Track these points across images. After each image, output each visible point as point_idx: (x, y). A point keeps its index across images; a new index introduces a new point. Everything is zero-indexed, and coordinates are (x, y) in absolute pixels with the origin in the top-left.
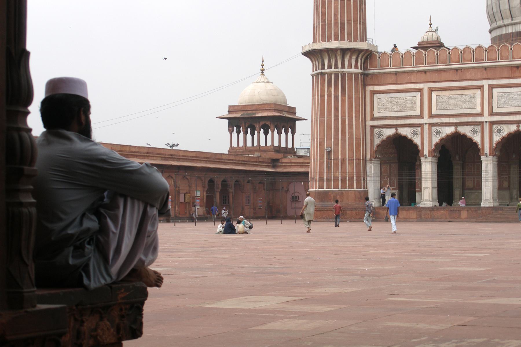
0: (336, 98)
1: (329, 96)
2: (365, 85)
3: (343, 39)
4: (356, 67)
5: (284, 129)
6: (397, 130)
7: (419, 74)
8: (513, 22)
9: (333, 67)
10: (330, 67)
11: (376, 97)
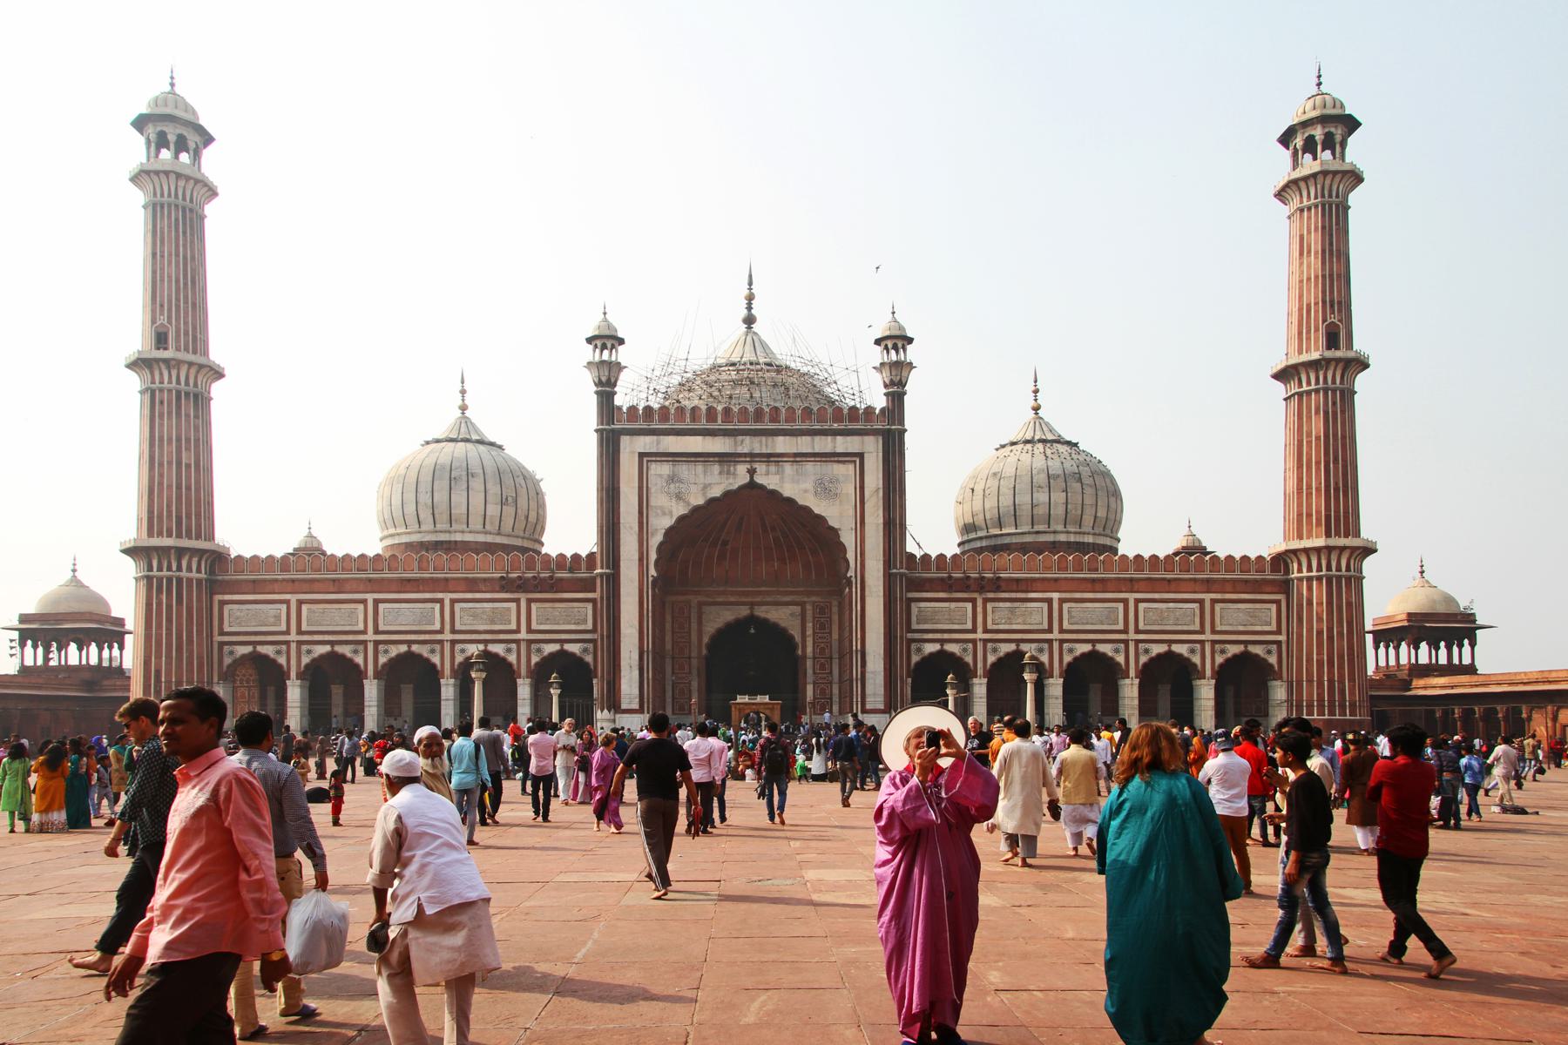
0: (169, 607)
2: (212, 594)
7: (284, 583)
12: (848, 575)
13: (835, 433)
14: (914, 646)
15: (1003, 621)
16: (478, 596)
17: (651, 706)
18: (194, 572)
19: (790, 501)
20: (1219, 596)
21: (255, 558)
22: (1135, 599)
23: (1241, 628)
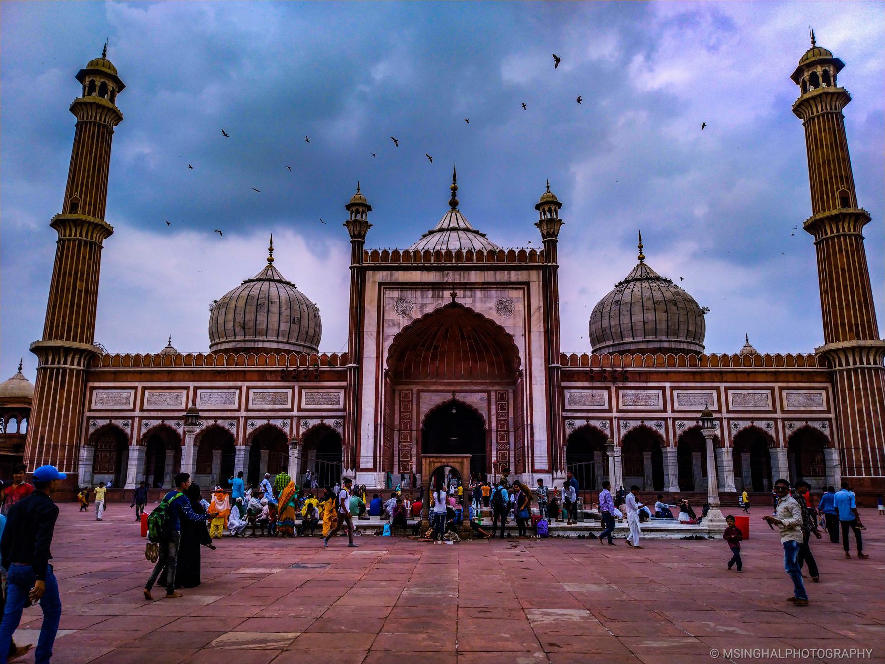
2: (87, 381)
3: (68, 339)
4: (79, 365)
6: (111, 421)
9: (56, 364)
10: (53, 363)
11: (95, 392)
12: (520, 369)
13: (510, 268)
14: (567, 422)
16: (266, 384)
17: (381, 465)
18: (75, 365)
19: (480, 316)
21: (118, 355)
22: (725, 387)
23: (802, 409)
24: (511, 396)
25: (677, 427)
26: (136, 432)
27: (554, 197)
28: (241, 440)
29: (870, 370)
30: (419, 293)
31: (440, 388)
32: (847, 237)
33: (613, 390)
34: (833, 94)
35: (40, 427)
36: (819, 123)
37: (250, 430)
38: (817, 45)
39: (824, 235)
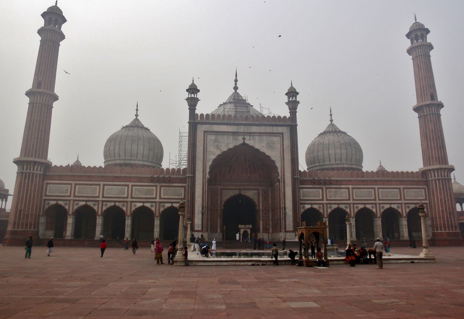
1: (25, 183)
2: (44, 180)
5: (1, 199)
6: (57, 202)
8: (115, 159)
12: (279, 178)
15: (333, 196)
16: (142, 184)
17: (206, 228)
19: (258, 150)
20: (405, 186)
21: (61, 166)
23: (414, 198)
24: (270, 192)
25: (355, 208)
26: (71, 209)
27: (295, 89)
28: (129, 213)
29: (445, 179)
30: (225, 137)
31: (232, 187)
32: (434, 115)
33: (324, 189)
34: (426, 45)
35: (19, 205)
36: (420, 59)
37: (133, 209)
38: (417, 21)
39: (423, 113)
